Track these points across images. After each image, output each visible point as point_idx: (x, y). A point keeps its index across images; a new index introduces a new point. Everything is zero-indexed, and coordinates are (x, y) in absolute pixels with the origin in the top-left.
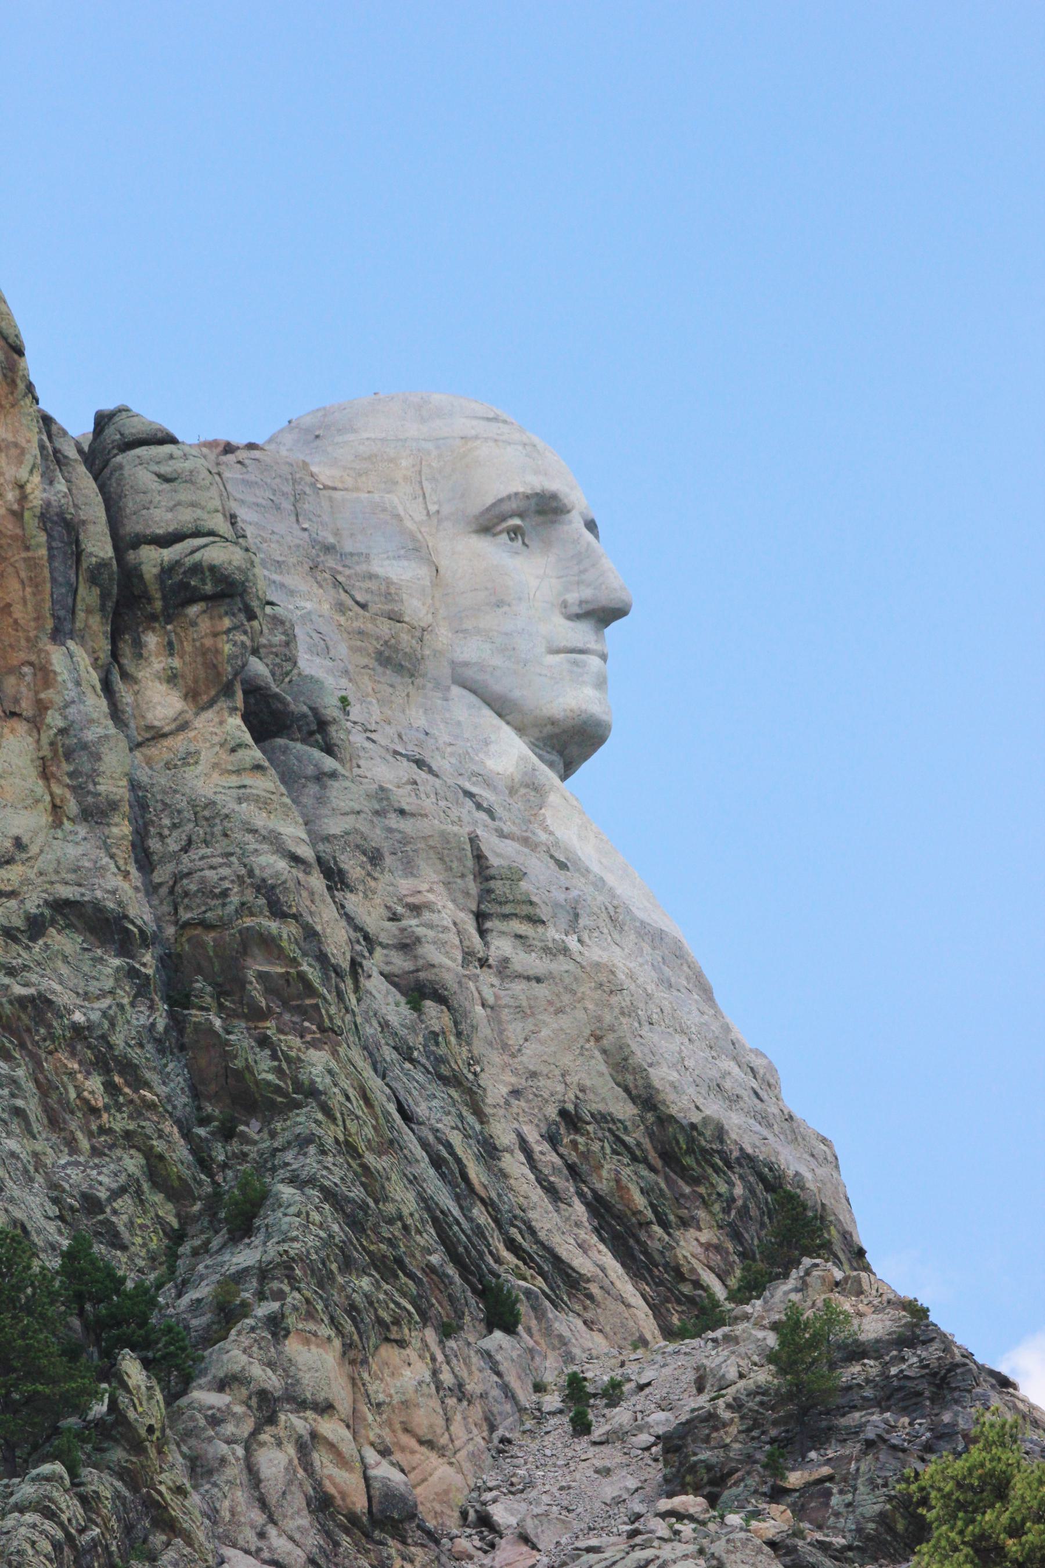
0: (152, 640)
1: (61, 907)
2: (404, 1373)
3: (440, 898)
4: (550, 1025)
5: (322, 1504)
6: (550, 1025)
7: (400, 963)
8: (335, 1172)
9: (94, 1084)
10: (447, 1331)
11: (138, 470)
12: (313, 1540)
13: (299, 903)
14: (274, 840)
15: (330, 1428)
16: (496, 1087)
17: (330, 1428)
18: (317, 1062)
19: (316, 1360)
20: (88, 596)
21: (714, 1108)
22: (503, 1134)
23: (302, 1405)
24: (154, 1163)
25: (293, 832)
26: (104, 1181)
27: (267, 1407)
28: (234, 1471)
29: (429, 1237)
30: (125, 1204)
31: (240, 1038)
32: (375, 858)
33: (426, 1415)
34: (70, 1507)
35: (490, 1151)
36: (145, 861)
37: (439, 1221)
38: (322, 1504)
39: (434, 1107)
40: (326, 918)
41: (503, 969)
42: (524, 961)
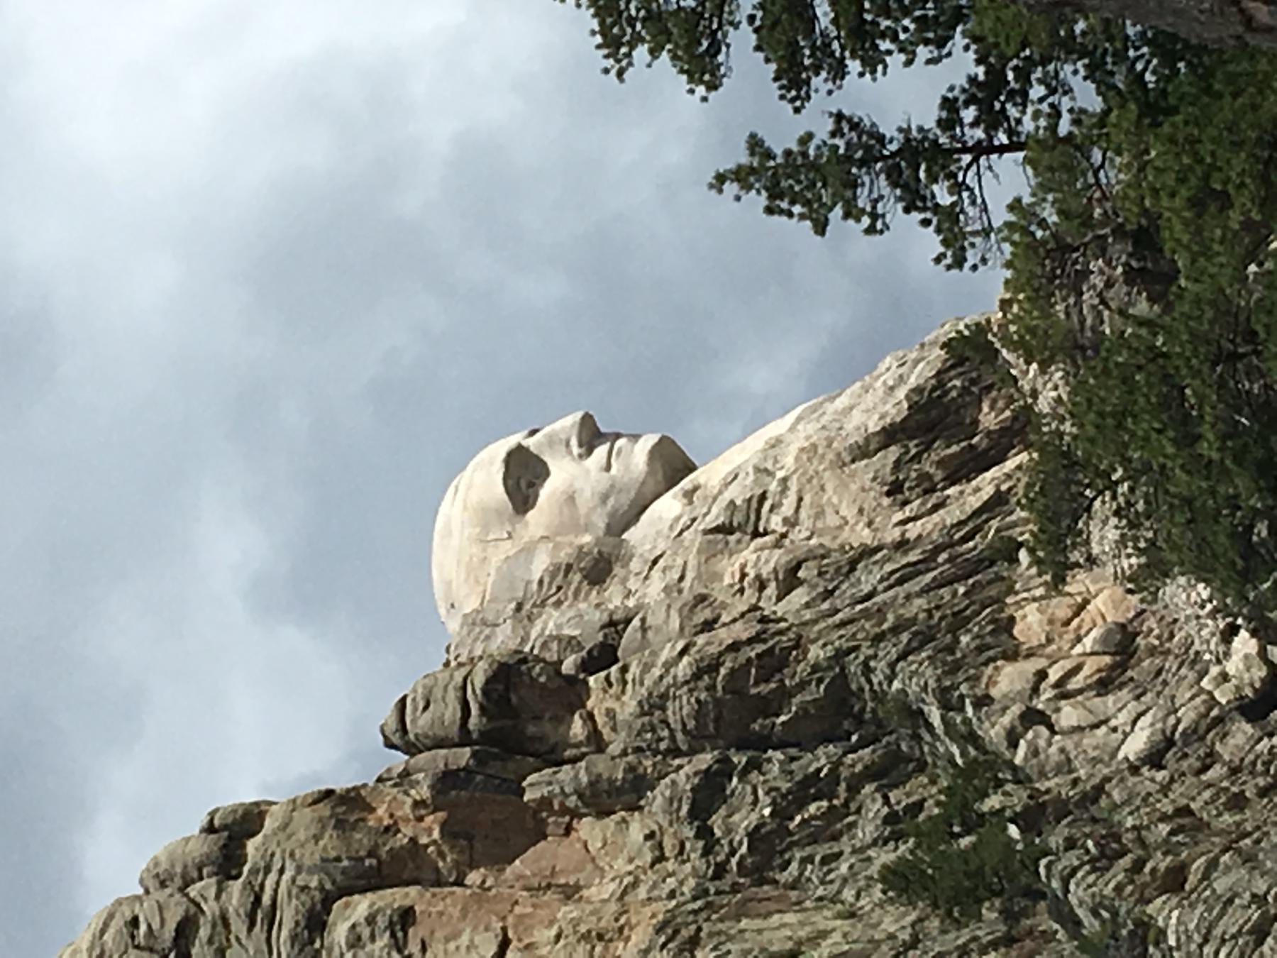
0: (531, 729)
3: (738, 560)
5: (1104, 685)
7: (771, 590)
8: (890, 650)
10: (1011, 591)
11: (419, 723)
12: (1125, 694)
14: (668, 666)
15: (1054, 674)
16: (864, 536)
18: (816, 653)
19: (1009, 679)
20: (494, 768)
21: (901, 393)
22: (896, 534)
24: (871, 773)
28: (1069, 744)
29: (945, 592)
34: (1071, 858)
35: (902, 545)
36: (675, 752)
37: (938, 584)
38: (1104, 685)
39: (867, 578)
40: (724, 636)
41: (791, 523)
42: (788, 508)
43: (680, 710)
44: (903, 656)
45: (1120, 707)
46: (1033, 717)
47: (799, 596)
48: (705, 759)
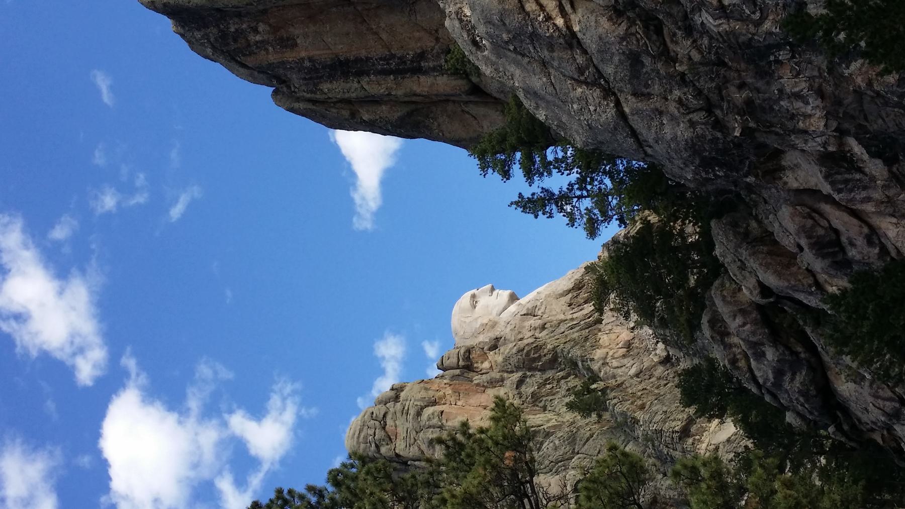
1: (517, 388)
2: (604, 339)
4: (554, 306)
6: (554, 306)
7: (538, 330)
8: (568, 346)
9: (548, 386)
10: (600, 330)
12: (630, 359)
13: (522, 346)
14: (511, 349)
15: (611, 353)
16: (562, 317)
17: (611, 353)
18: (549, 347)
19: (598, 354)
21: (573, 280)
22: (570, 317)
23: (606, 358)
24: (563, 378)
25: (511, 345)
26: (564, 387)
27: (605, 364)
28: (615, 371)
30: (569, 384)
31: (544, 359)
32: (520, 332)
33: (613, 336)
35: (572, 319)
36: (512, 372)
38: (624, 356)
39: (563, 328)
40: (525, 342)
42: (542, 310)
43: (513, 361)
44: (572, 348)
45: (627, 361)
46: (605, 364)
47: (545, 332)
48: (520, 374)
